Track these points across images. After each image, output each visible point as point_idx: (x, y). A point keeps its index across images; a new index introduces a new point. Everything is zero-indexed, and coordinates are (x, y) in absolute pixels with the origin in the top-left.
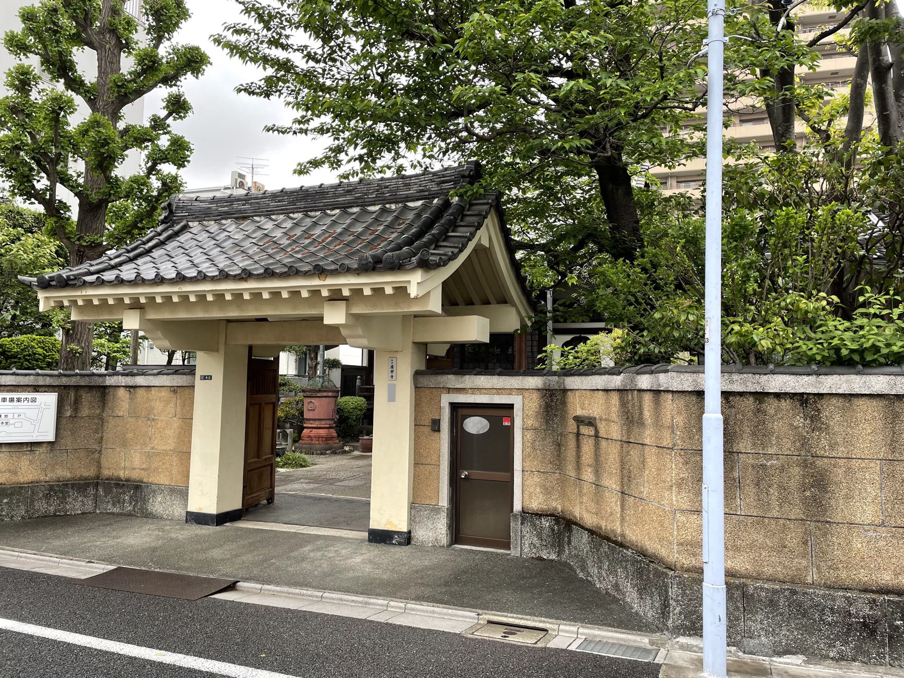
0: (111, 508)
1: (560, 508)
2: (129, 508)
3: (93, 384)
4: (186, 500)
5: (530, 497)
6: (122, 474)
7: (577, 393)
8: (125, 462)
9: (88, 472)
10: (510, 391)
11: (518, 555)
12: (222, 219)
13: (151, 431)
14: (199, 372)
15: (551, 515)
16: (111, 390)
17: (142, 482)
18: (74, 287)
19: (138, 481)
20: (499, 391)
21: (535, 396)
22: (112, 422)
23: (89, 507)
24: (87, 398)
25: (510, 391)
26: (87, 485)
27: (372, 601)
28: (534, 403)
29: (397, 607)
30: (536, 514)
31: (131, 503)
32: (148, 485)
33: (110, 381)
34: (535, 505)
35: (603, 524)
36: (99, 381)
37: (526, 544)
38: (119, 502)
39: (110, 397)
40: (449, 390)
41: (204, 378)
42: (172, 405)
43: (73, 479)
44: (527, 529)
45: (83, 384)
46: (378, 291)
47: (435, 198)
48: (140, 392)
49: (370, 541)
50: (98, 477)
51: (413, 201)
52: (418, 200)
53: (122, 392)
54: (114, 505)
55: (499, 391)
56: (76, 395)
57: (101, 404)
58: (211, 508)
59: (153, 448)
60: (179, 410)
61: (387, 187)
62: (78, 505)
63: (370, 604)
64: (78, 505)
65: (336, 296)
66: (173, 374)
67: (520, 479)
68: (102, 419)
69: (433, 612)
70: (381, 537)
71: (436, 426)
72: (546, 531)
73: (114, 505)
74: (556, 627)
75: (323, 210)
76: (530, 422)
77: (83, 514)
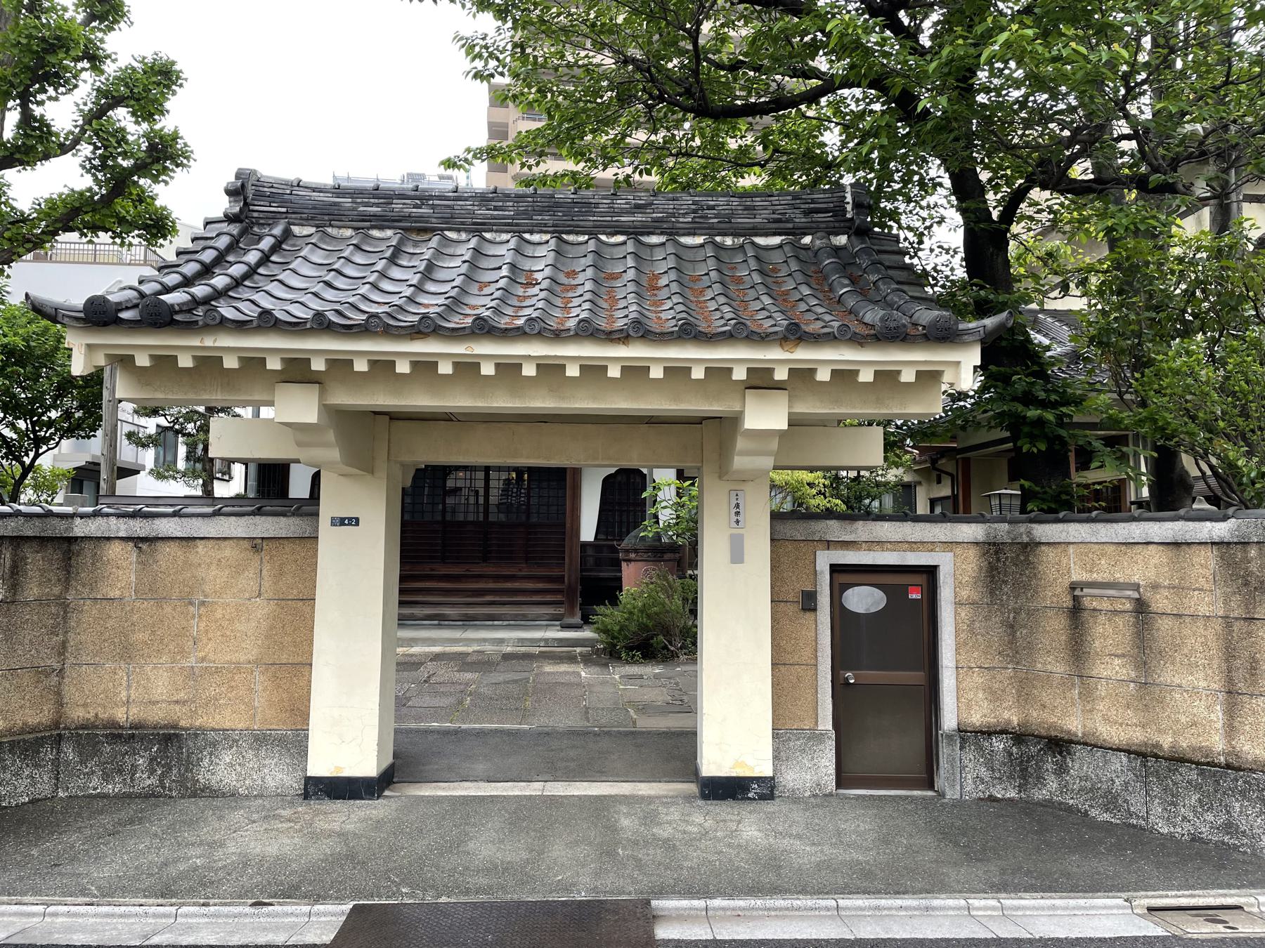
0: (96, 785)
1: (1015, 720)
2: (146, 781)
3: (49, 533)
4: (303, 753)
5: (969, 707)
6: (120, 715)
7: (1071, 549)
8: (131, 689)
9: (37, 715)
10: (930, 546)
11: (957, 796)
12: (373, 227)
13: (196, 627)
14: (327, 509)
15: (1002, 732)
16: (86, 545)
17: (175, 727)
18: (190, 327)
19: (165, 727)
20: (913, 545)
21: (972, 553)
22: (90, 612)
23: (44, 786)
24: (35, 560)
25: (930, 546)
26: (39, 742)
27: (936, 903)
28: (971, 563)
29: (986, 908)
30: (983, 733)
31: (152, 772)
32: (197, 733)
33: (80, 528)
34: (978, 717)
35: (1157, 738)
36: (59, 528)
37: (963, 777)
38: (120, 772)
39: (86, 558)
40: (829, 545)
41: (342, 522)
42: (250, 573)
43: (10, 732)
44: (969, 756)
45: (30, 533)
46: (887, 378)
47: (806, 234)
48: (167, 549)
49: (705, 797)
50: (56, 724)
51: (766, 235)
52: (775, 234)
53: (115, 551)
54: (106, 777)
55: (913, 545)
56: (14, 555)
57: (62, 574)
58: (367, 766)
59: (203, 659)
60: (266, 584)
61: (713, 208)
62: (22, 784)
63: (934, 909)
64: (22, 784)
65: (760, 381)
66: (253, 514)
67: (953, 681)
68: (65, 606)
69: (1054, 907)
70: (728, 789)
71: (809, 602)
72: (1000, 757)
73: (106, 777)
74: (1252, 900)
75: (593, 234)
76: (965, 593)
77: (31, 802)
